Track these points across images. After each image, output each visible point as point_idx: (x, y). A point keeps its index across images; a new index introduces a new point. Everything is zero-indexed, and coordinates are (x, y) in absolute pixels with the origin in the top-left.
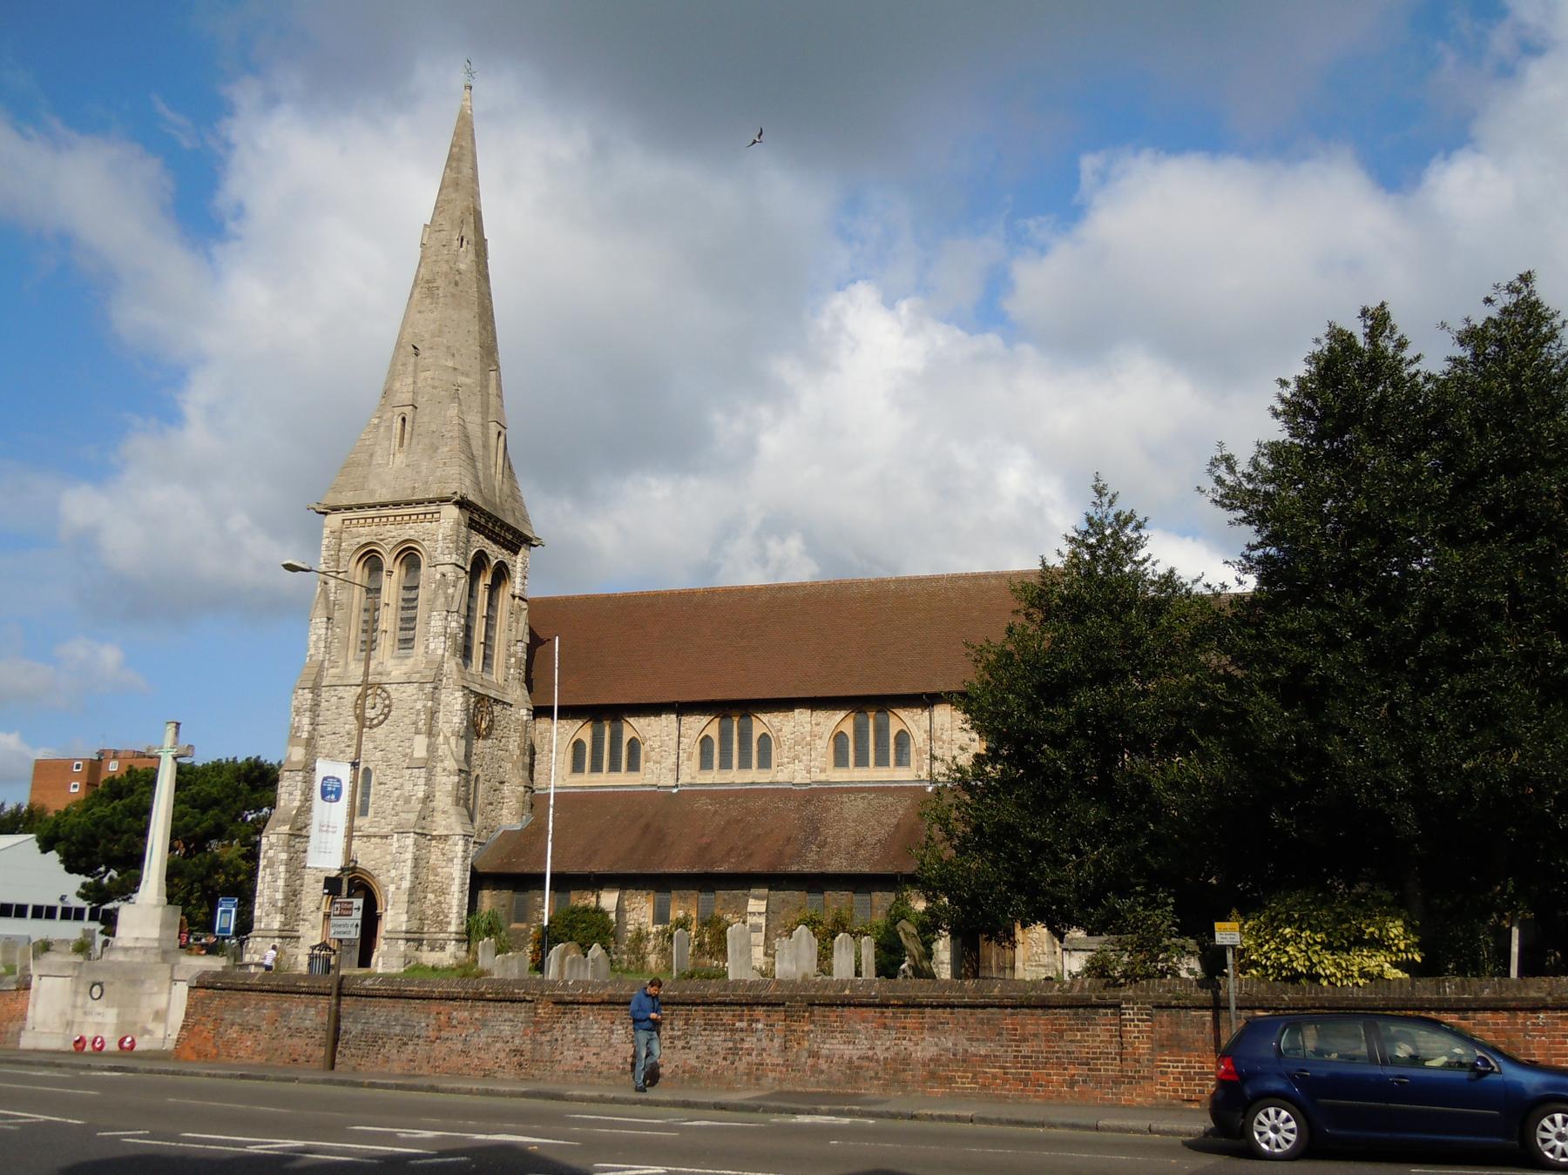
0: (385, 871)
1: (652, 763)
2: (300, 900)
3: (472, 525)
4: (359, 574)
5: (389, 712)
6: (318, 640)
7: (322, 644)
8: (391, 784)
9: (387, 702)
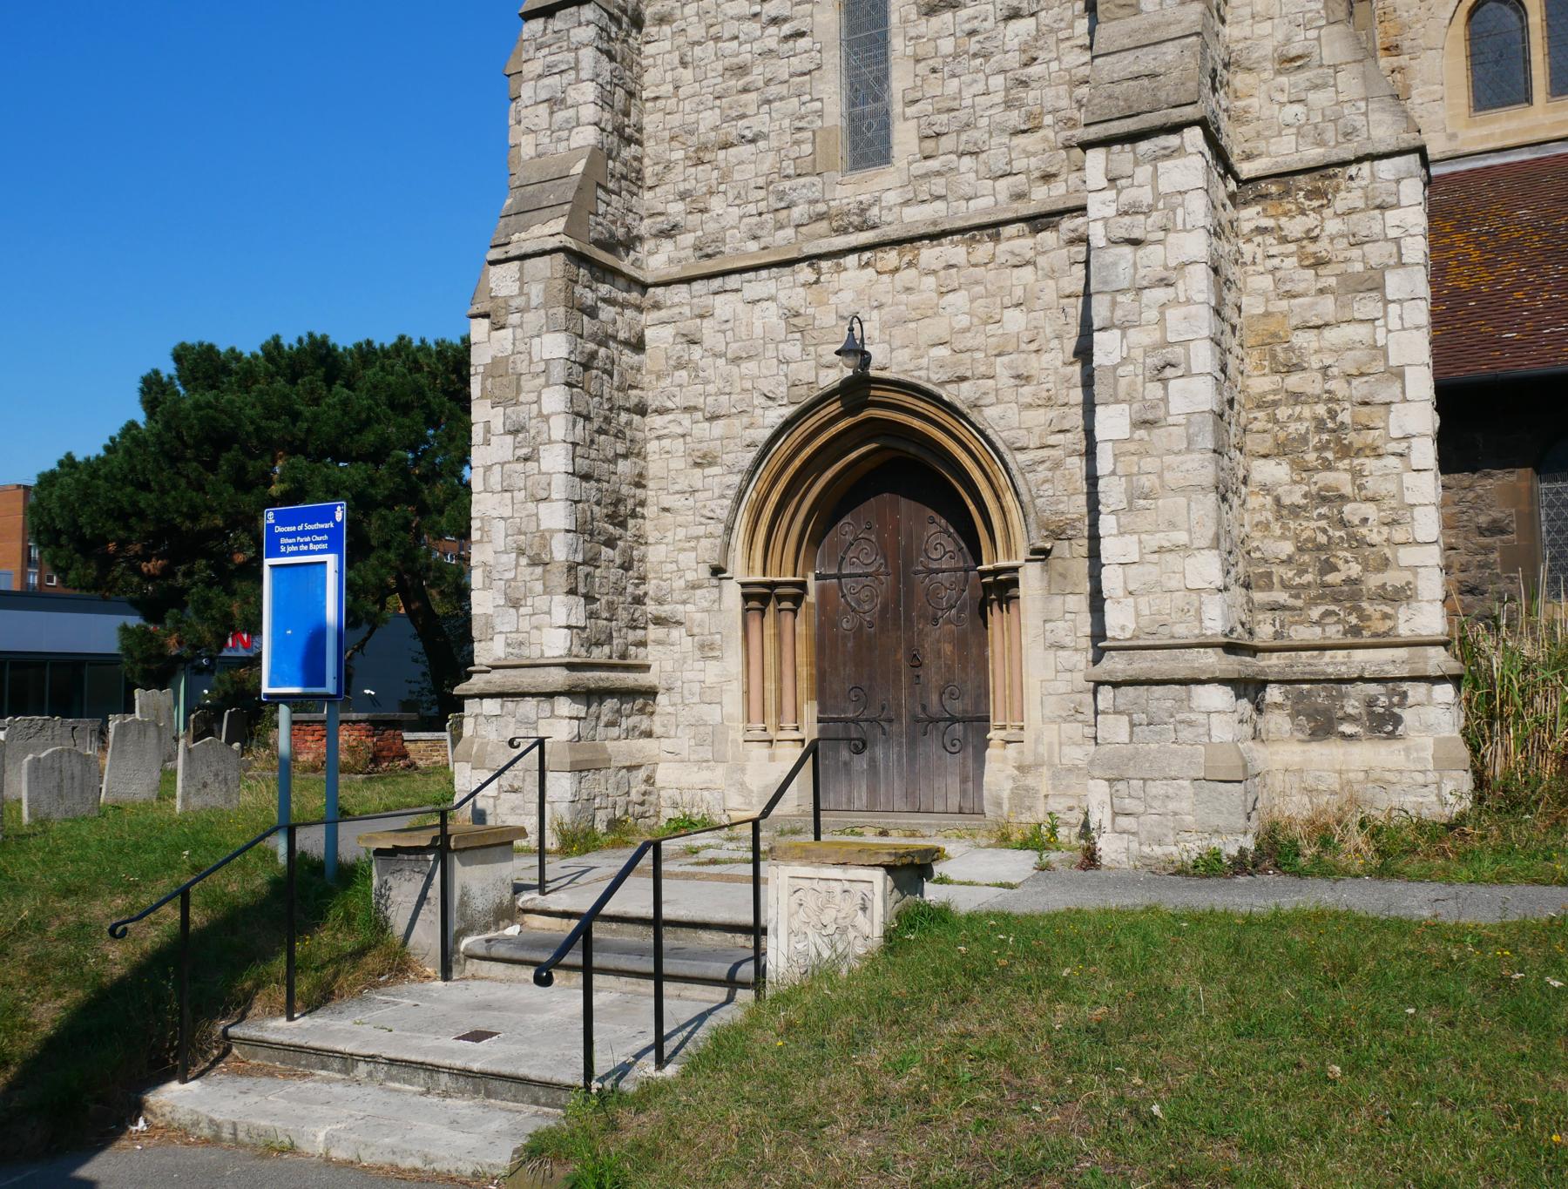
0: (1004, 379)
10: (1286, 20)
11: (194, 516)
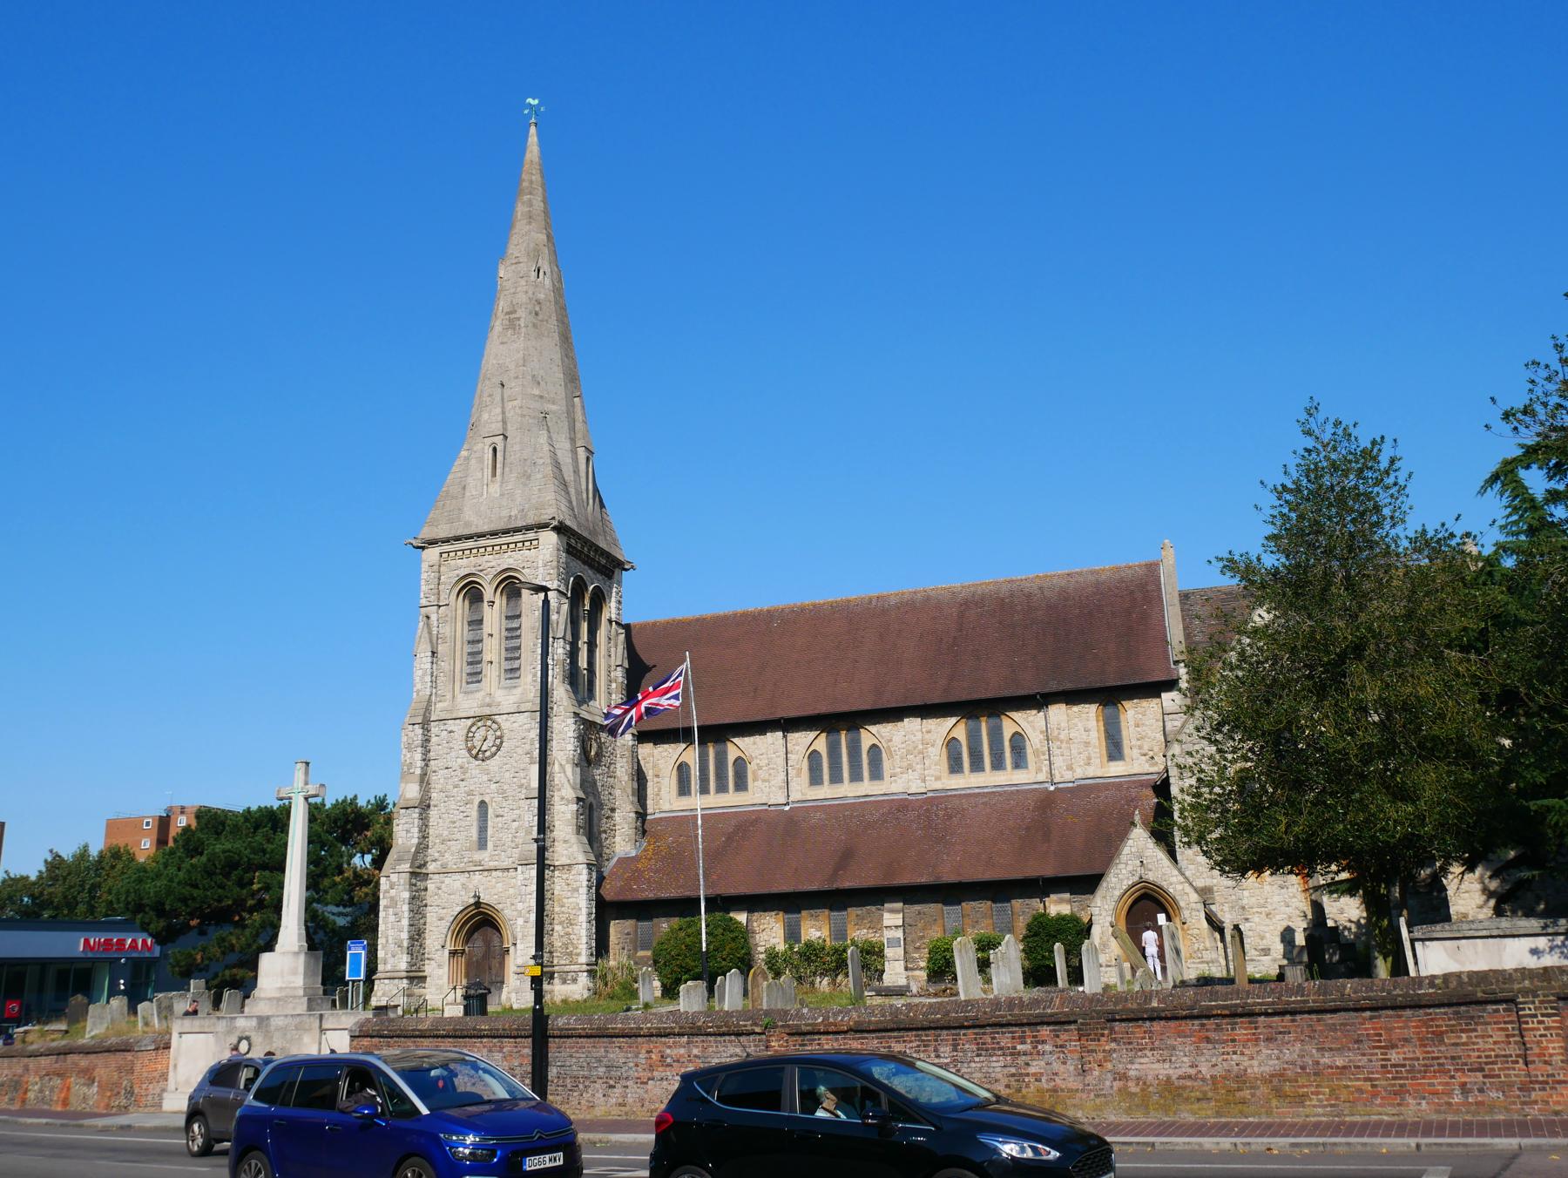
0: (509, 905)
1: (760, 782)
2: (424, 939)
3: (570, 551)
4: (461, 607)
5: (502, 743)
6: (424, 674)
7: (428, 678)
8: (508, 817)
9: (498, 733)
11: (219, 900)
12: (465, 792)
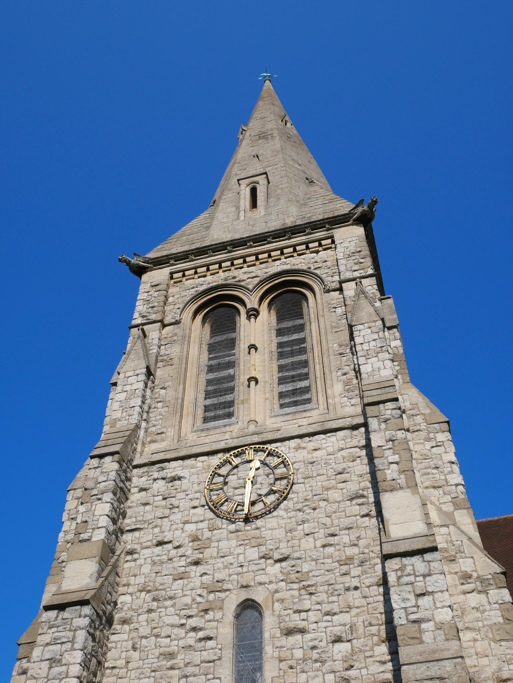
9: (281, 471)
10: (496, 658)
12: (203, 586)
